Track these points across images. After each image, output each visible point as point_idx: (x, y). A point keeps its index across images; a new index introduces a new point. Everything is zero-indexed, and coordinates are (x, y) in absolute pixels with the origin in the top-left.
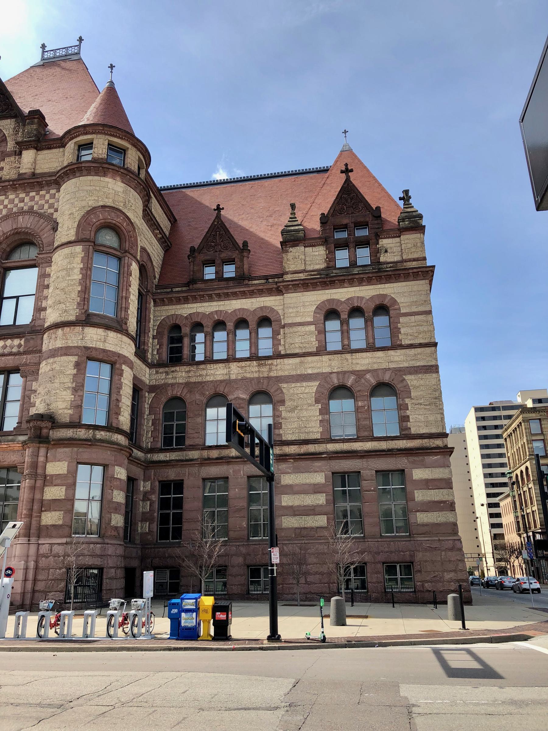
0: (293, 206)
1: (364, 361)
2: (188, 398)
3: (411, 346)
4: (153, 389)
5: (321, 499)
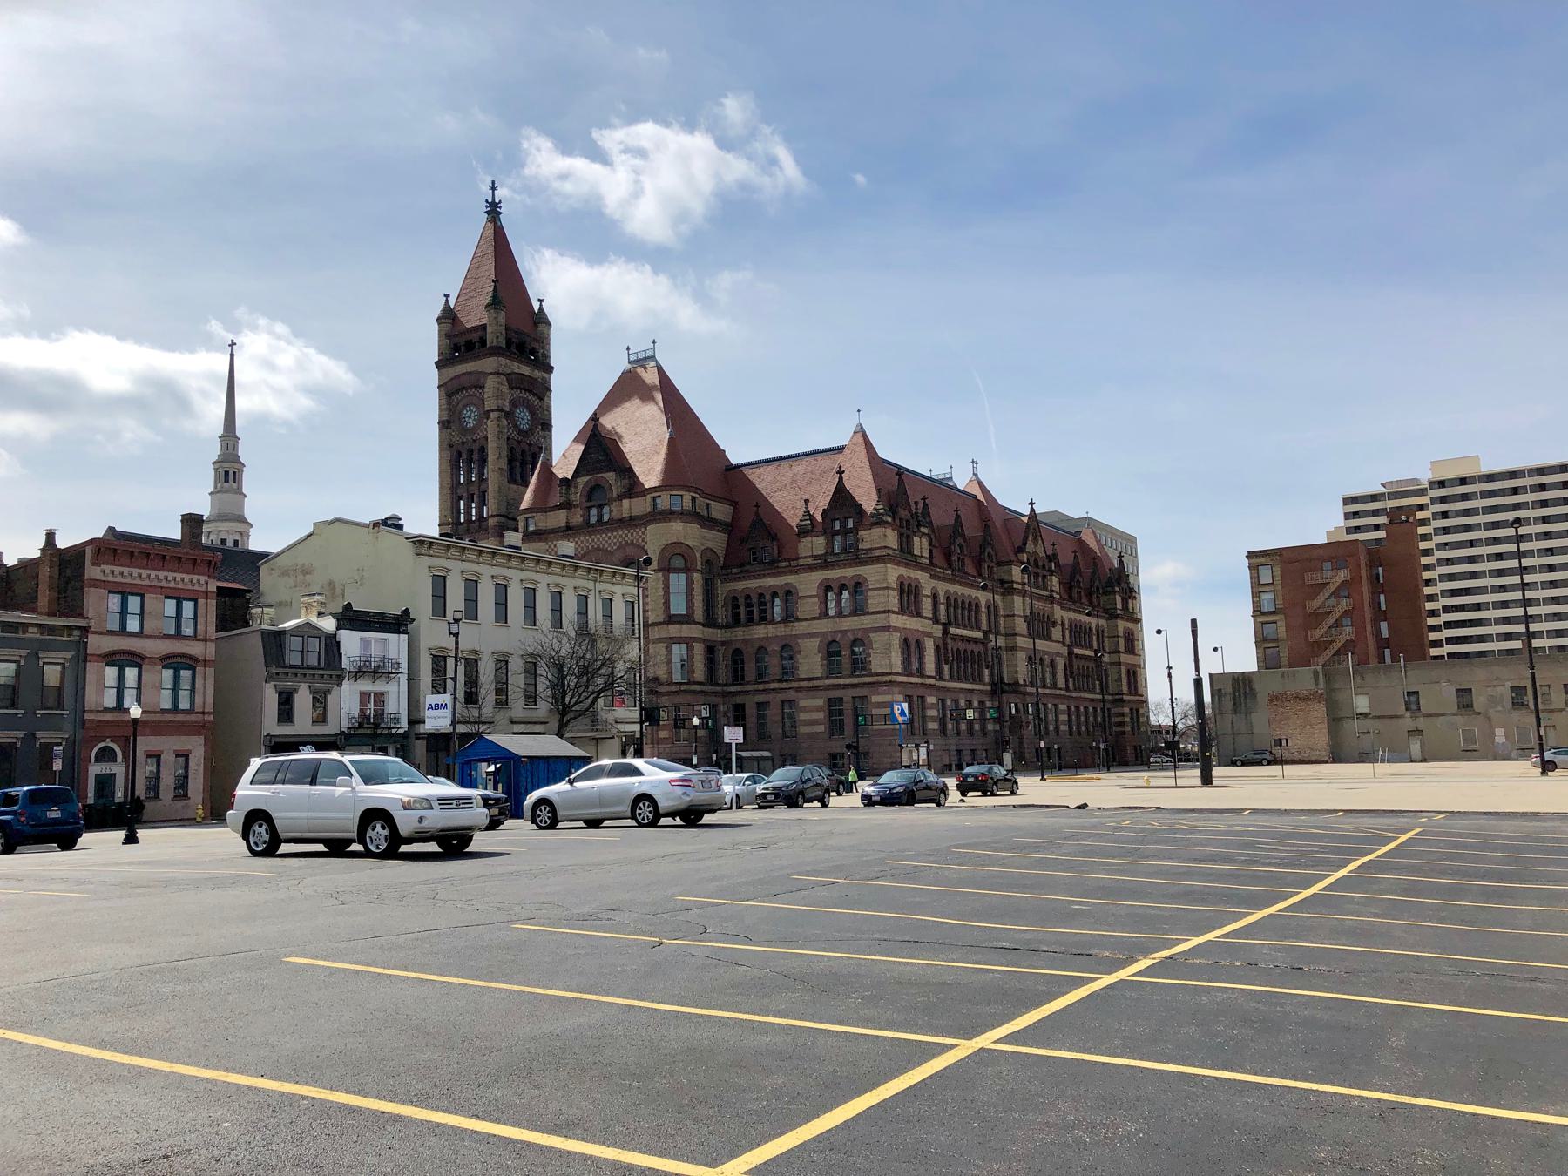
0: (807, 501)
1: (849, 623)
4: (723, 643)
5: (821, 715)
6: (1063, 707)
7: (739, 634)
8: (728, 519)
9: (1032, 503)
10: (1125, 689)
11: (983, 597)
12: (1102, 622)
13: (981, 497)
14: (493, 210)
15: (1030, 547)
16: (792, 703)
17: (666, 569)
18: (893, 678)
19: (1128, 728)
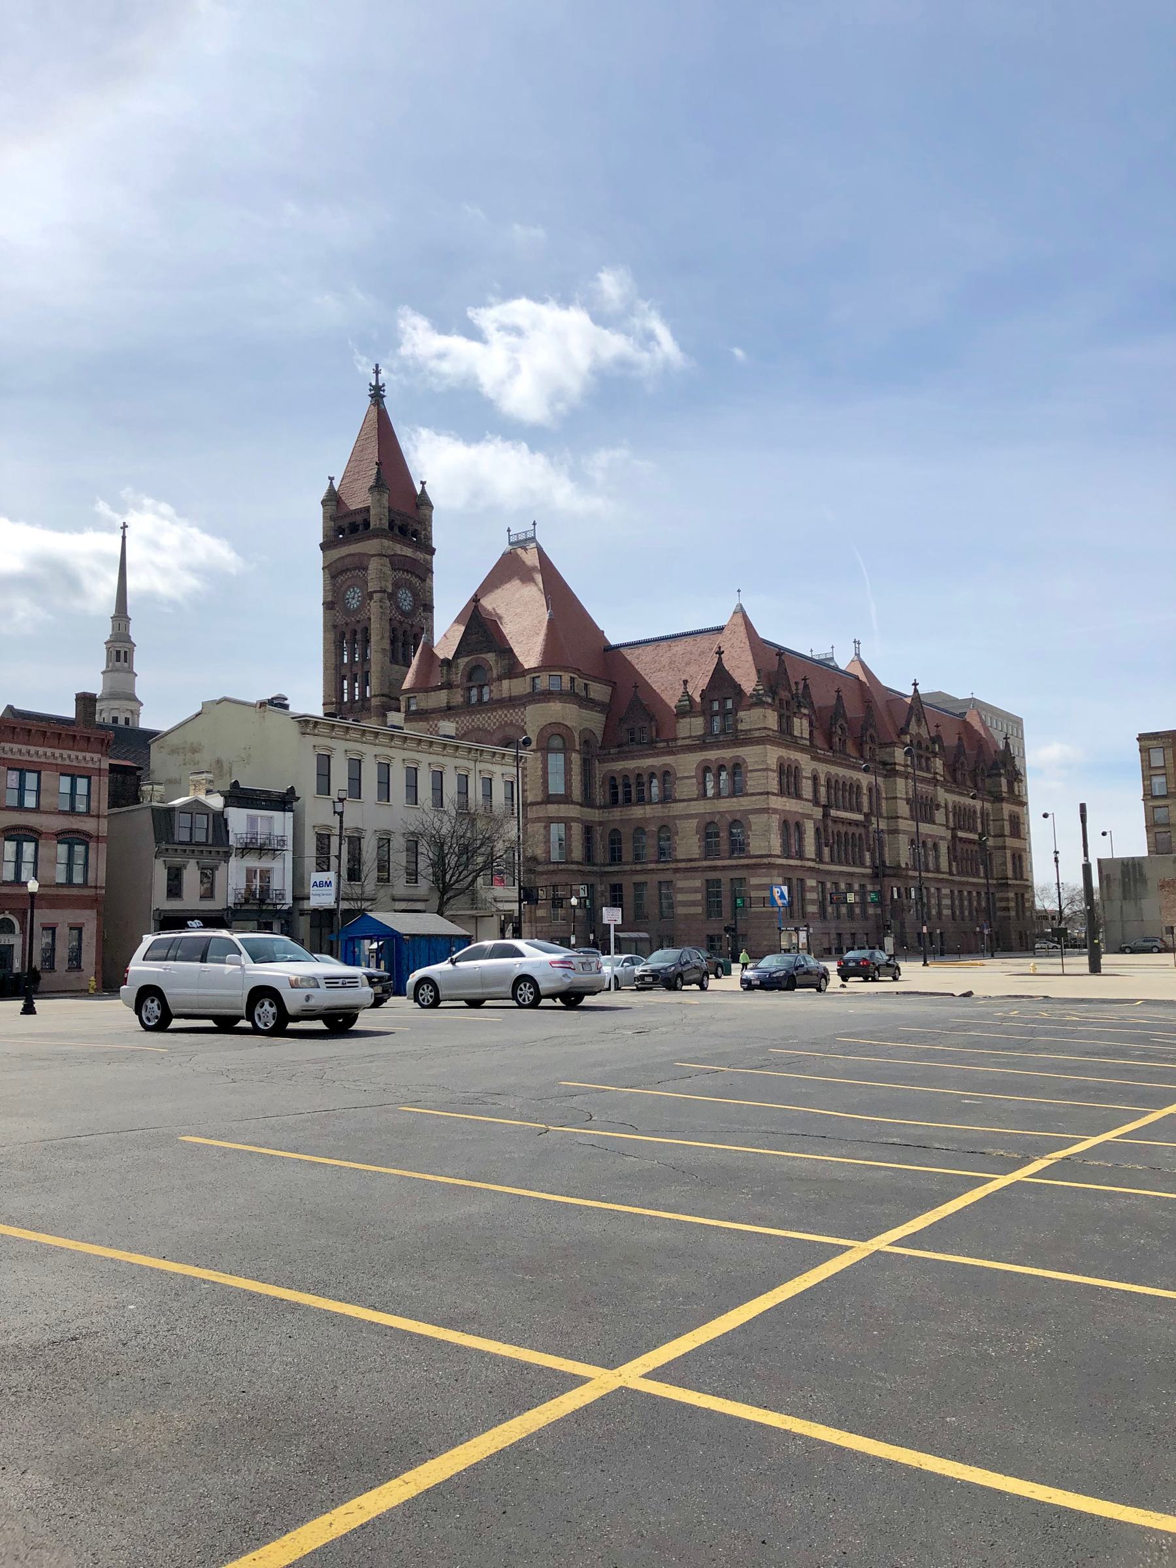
0: (685, 682)
1: (725, 805)
2: (622, 830)
3: (753, 794)
4: (601, 823)
5: (699, 897)
6: (945, 891)
7: (617, 814)
8: (607, 699)
9: (915, 684)
10: (1010, 874)
11: (865, 780)
12: (988, 805)
13: (863, 678)
14: (377, 394)
15: (913, 728)
16: (669, 883)
17: (545, 749)
18: (772, 860)
19: (1013, 913)
